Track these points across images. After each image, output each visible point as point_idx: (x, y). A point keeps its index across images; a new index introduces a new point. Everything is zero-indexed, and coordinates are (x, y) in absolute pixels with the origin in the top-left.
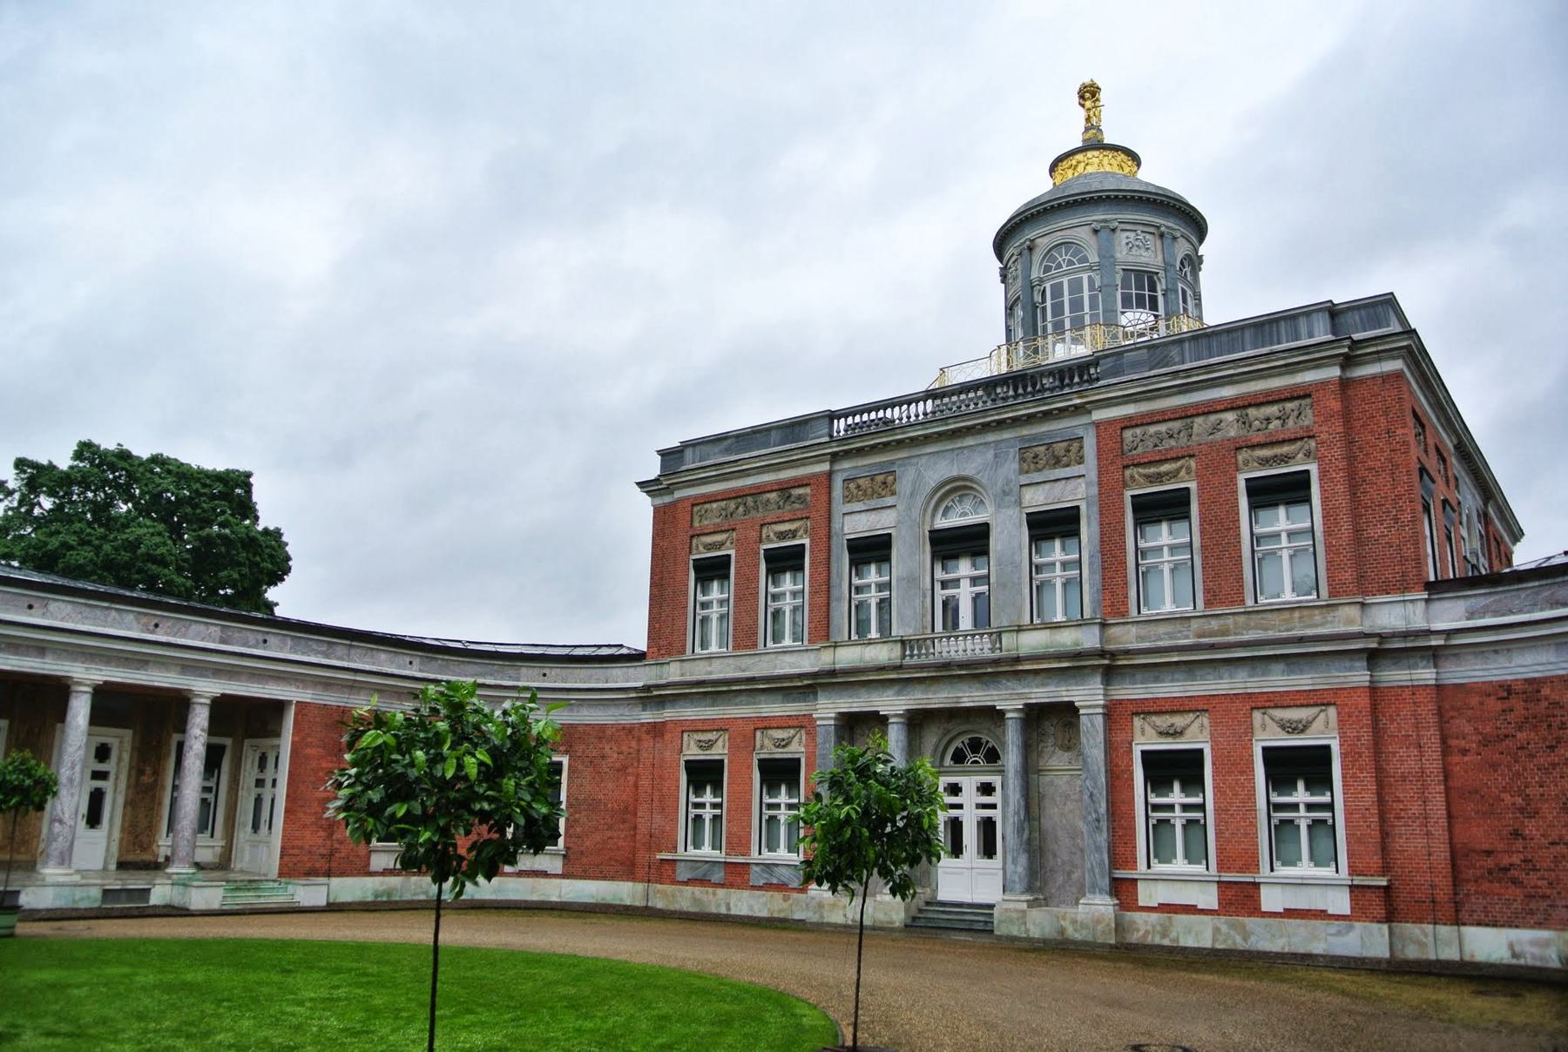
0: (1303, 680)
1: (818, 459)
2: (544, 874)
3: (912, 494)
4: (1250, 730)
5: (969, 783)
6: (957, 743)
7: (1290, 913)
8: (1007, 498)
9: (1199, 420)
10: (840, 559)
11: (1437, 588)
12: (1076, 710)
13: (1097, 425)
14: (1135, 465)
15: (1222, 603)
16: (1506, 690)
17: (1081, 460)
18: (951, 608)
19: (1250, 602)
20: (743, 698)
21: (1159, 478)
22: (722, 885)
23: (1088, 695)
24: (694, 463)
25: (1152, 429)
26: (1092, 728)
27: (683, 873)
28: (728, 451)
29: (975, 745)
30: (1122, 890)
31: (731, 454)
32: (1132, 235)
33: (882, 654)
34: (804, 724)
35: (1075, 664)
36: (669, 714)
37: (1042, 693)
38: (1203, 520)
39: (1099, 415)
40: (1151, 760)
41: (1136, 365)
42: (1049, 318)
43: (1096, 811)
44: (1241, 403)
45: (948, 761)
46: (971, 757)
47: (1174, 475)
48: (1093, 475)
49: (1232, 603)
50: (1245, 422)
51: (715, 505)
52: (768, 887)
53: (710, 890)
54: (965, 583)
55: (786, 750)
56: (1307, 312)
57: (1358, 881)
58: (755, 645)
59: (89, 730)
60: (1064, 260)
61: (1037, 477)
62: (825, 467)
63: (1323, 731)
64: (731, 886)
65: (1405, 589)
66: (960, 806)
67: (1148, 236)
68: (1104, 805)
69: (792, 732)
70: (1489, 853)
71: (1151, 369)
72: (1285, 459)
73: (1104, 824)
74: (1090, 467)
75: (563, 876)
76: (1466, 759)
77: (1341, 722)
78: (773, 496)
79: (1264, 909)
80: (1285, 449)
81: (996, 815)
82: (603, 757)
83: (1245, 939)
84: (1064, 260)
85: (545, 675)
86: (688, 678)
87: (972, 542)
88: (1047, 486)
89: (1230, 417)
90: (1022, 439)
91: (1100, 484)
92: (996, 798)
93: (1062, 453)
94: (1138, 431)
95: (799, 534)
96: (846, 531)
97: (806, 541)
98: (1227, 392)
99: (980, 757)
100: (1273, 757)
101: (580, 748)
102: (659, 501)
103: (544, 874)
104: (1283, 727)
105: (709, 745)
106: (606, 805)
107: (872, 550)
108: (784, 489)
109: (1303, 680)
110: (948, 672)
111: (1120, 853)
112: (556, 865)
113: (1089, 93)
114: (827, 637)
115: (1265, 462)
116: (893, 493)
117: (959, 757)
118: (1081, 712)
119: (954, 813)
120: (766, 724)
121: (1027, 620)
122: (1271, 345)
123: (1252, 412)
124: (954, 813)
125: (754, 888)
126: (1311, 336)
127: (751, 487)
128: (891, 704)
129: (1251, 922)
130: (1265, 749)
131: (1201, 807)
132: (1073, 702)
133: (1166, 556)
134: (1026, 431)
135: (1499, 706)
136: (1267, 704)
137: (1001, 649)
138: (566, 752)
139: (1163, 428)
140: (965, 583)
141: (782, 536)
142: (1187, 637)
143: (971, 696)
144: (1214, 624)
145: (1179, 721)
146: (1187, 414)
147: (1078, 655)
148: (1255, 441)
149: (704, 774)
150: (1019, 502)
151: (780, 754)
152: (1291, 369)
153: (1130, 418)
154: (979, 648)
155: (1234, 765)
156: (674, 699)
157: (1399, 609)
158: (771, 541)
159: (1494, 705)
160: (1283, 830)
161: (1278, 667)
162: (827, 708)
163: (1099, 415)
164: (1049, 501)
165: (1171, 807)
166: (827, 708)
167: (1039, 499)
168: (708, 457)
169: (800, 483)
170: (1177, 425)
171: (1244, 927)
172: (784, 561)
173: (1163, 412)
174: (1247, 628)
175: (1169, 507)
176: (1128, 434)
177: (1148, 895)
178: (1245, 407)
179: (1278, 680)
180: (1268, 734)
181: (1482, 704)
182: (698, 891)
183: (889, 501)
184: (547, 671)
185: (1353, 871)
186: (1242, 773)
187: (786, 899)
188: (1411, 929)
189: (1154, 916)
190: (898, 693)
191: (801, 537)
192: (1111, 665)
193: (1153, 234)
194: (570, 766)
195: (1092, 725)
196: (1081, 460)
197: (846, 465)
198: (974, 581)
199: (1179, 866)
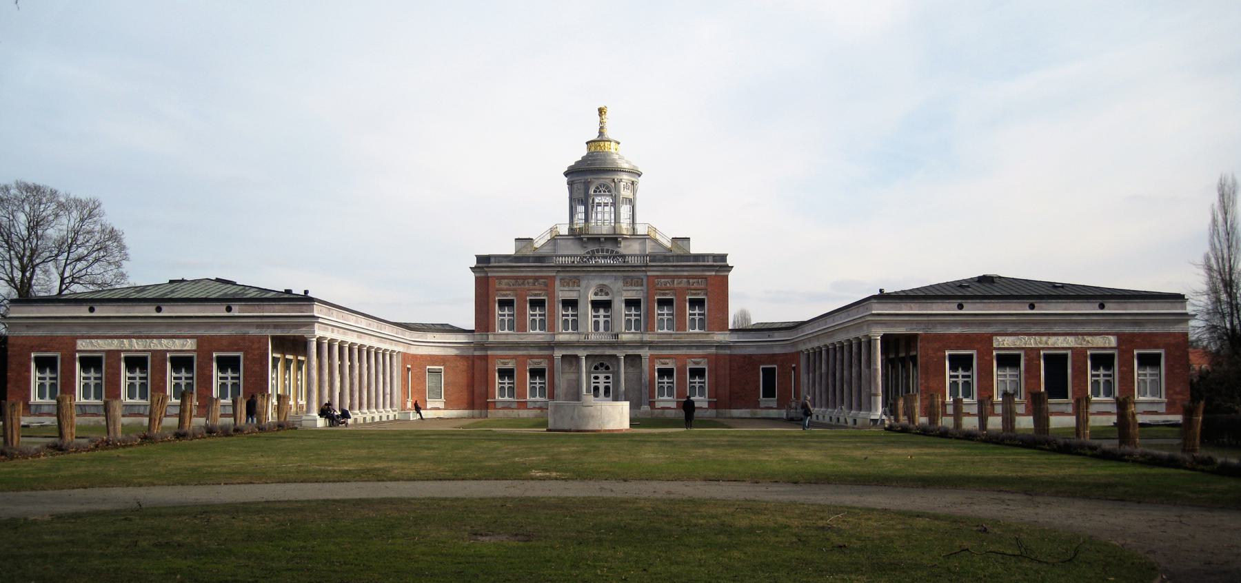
0: (700, 352)
1: (552, 271)
2: (439, 409)
3: (586, 288)
5: (602, 376)
13: (648, 276)
16: (744, 356)
20: (522, 348)
21: (664, 294)
22: (516, 409)
23: (645, 353)
24: (495, 263)
25: (663, 280)
26: (646, 364)
27: (499, 405)
28: (511, 261)
29: (602, 365)
30: (652, 404)
33: (574, 338)
34: (551, 359)
35: (642, 344)
36: (489, 353)
37: (630, 352)
38: (677, 307)
39: (648, 274)
40: (660, 371)
41: (660, 261)
45: (592, 369)
47: (668, 294)
48: (645, 290)
50: (689, 282)
52: (534, 408)
53: (511, 410)
54: (602, 317)
56: (708, 255)
57: (710, 400)
61: (629, 288)
62: (554, 274)
63: (703, 365)
64: (519, 409)
66: (599, 383)
69: (542, 360)
70: (737, 393)
74: (644, 288)
75: (444, 409)
77: (708, 363)
80: (698, 292)
87: (607, 305)
88: (631, 292)
89: (685, 280)
90: (624, 276)
91: (647, 293)
92: (611, 380)
98: (686, 274)
101: (448, 364)
102: (478, 275)
103: (439, 409)
105: (508, 363)
107: (571, 304)
108: (536, 279)
109: (700, 352)
110: (602, 345)
111: (652, 395)
112: (442, 405)
113: (601, 111)
114: (554, 331)
116: (579, 286)
117: (596, 368)
119: (597, 384)
120: (532, 357)
123: (691, 281)
124: (597, 384)
126: (708, 262)
127: (523, 276)
128: (582, 353)
130: (690, 369)
131: (704, 383)
133: (665, 316)
134: (625, 274)
139: (666, 280)
140: (602, 317)
141: (535, 295)
143: (609, 352)
145: (667, 361)
146: (673, 277)
147: (642, 342)
149: (506, 373)
150: (622, 295)
151: (537, 367)
152: (703, 271)
153: (658, 276)
154: (606, 338)
156: (492, 348)
157: (723, 336)
158: (531, 296)
161: (695, 348)
162: (558, 354)
163: (648, 274)
165: (664, 383)
166: (558, 354)
168: (502, 262)
169: (542, 277)
170: (669, 280)
173: (668, 276)
175: (668, 303)
177: (658, 405)
179: (694, 352)
182: (506, 411)
183: (579, 288)
185: (709, 397)
187: (542, 411)
188: (720, 411)
189: (659, 410)
190: (584, 350)
191: (543, 296)
192: (651, 345)
196: (642, 285)
197: (561, 274)
199: (666, 398)
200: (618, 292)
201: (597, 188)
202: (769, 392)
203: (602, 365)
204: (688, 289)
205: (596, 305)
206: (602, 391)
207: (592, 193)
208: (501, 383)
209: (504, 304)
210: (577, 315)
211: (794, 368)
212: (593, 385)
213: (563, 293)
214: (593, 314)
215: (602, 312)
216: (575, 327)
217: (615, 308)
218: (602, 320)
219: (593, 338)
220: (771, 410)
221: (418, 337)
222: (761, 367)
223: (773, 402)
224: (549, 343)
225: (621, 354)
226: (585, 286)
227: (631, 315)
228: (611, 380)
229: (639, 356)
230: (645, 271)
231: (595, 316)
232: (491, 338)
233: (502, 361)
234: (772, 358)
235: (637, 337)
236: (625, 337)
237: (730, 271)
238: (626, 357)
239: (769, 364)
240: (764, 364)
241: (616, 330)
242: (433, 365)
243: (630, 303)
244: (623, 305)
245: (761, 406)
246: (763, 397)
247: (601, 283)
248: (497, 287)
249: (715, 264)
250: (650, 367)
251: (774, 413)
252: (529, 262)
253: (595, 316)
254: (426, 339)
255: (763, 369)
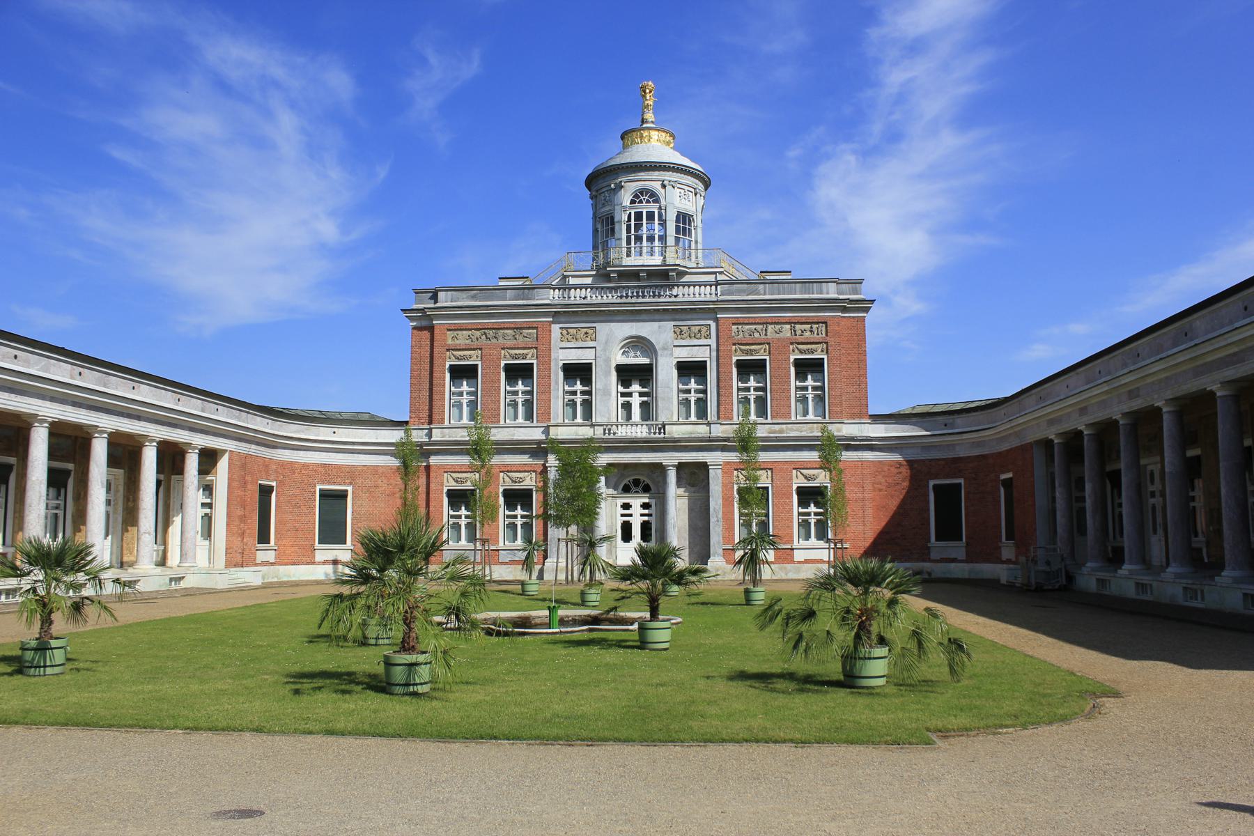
3: (606, 343)
4: (791, 479)
6: (626, 482)
7: (807, 561)
8: (666, 352)
9: (770, 327)
10: (557, 375)
11: (878, 418)
12: (708, 466)
14: (739, 344)
15: (781, 417)
17: (708, 336)
18: (627, 407)
19: (793, 418)
25: (747, 327)
28: (474, 298)
29: (636, 482)
31: (476, 301)
32: (683, 191)
36: (434, 460)
42: (633, 232)
43: (717, 517)
44: (794, 321)
46: (634, 489)
47: (757, 351)
48: (714, 346)
49: (786, 418)
51: (464, 332)
54: (636, 395)
55: (521, 484)
58: (498, 421)
59: (108, 471)
60: (644, 199)
65: (861, 418)
66: (631, 515)
67: (690, 193)
68: (721, 513)
71: (747, 295)
72: (812, 352)
73: (721, 523)
74: (712, 342)
76: (881, 493)
78: (509, 332)
79: (796, 559)
80: (813, 346)
81: (653, 520)
82: (376, 487)
83: (786, 574)
84: (644, 199)
85: (334, 433)
86: (447, 439)
93: (696, 331)
94: (740, 327)
95: (528, 357)
96: (561, 358)
97: (535, 362)
99: (639, 489)
100: (801, 491)
101: (359, 481)
104: (806, 478)
106: (379, 517)
107: (579, 372)
115: (801, 352)
118: (710, 467)
121: (675, 419)
122: (809, 294)
123: (798, 327)
125: (502, 563)
126: (828, 293)
129: (789, 566)
132: (706, 462)
133: (752, 392)
135: (896, 471)
136: (800, 467)
137: (664, 433)
138: (351, 483)
139: (754, 327)
140: (636, 395)
141: (515, 357)
142: (763, 433)
144: (777, 427)
148: (800, 341)
150: (672, 354)
154: (641, 432)
155: (784, 494)
156: (437, 453)
159: (893, 469)
160: (805, 525)
164: (690, 356)
167: (685, 354)
171: (785, 568)
172: (518, 372)
174: (792, 430)
176: (734, 327)
178: (795, 323)
180: (798, 481)
181: (889, 470)
184: (335, 430)
186: (788, 498)
193: (692, 192)
194: (353, 492)
195: (716, 474)
196: (708, 336)
198: (641, 394)
200: (664, 349)
201: (636, 196)
202: (948, 530)
203: (636, 482)
204: (792, 343)
205: (626, 374)
206: (636, 531)
207: (628, 204)
208: (453, 517)
209: (463, 373)
210: (589, 393)
211: (1008, 484)
212: (620, 520)
213: (564, 354)
214: (621, 389)
215: (636, 388)
216: (588, 414)
217: (660, 377)
218: (636, 401)
219: (623, 432)
220: (953, 565)
221: (295, 432)
222: (932, 483)
223: (957, 549)
224: (539, 442)
225: (670, 459)
226: (604, 341)
227: (688, 391)
228: (653, 510)
229: (704, 466)
230: (714, 311)
231: (623, 395)
232: (437, 435)
233: (455, 475)
234: (954, 465)
235: (702, 430)
236: (675, 431)
237: (867, 310)
238: (680, 467)
239: (947, 477)
240: (936, 478)
241: (662, 418)
242: (329, 483)
243: (691, 370)
244: (675, 372)
245: (933, 555)
246: (937, 540)
247: (634, 333)
248: (450, 342)
249: (841, 297)
250: (724, 485)
251: (960, 570)
252: (505, 299)
253: (623, 395)
254: (318, 435)
255: (935, 487)
